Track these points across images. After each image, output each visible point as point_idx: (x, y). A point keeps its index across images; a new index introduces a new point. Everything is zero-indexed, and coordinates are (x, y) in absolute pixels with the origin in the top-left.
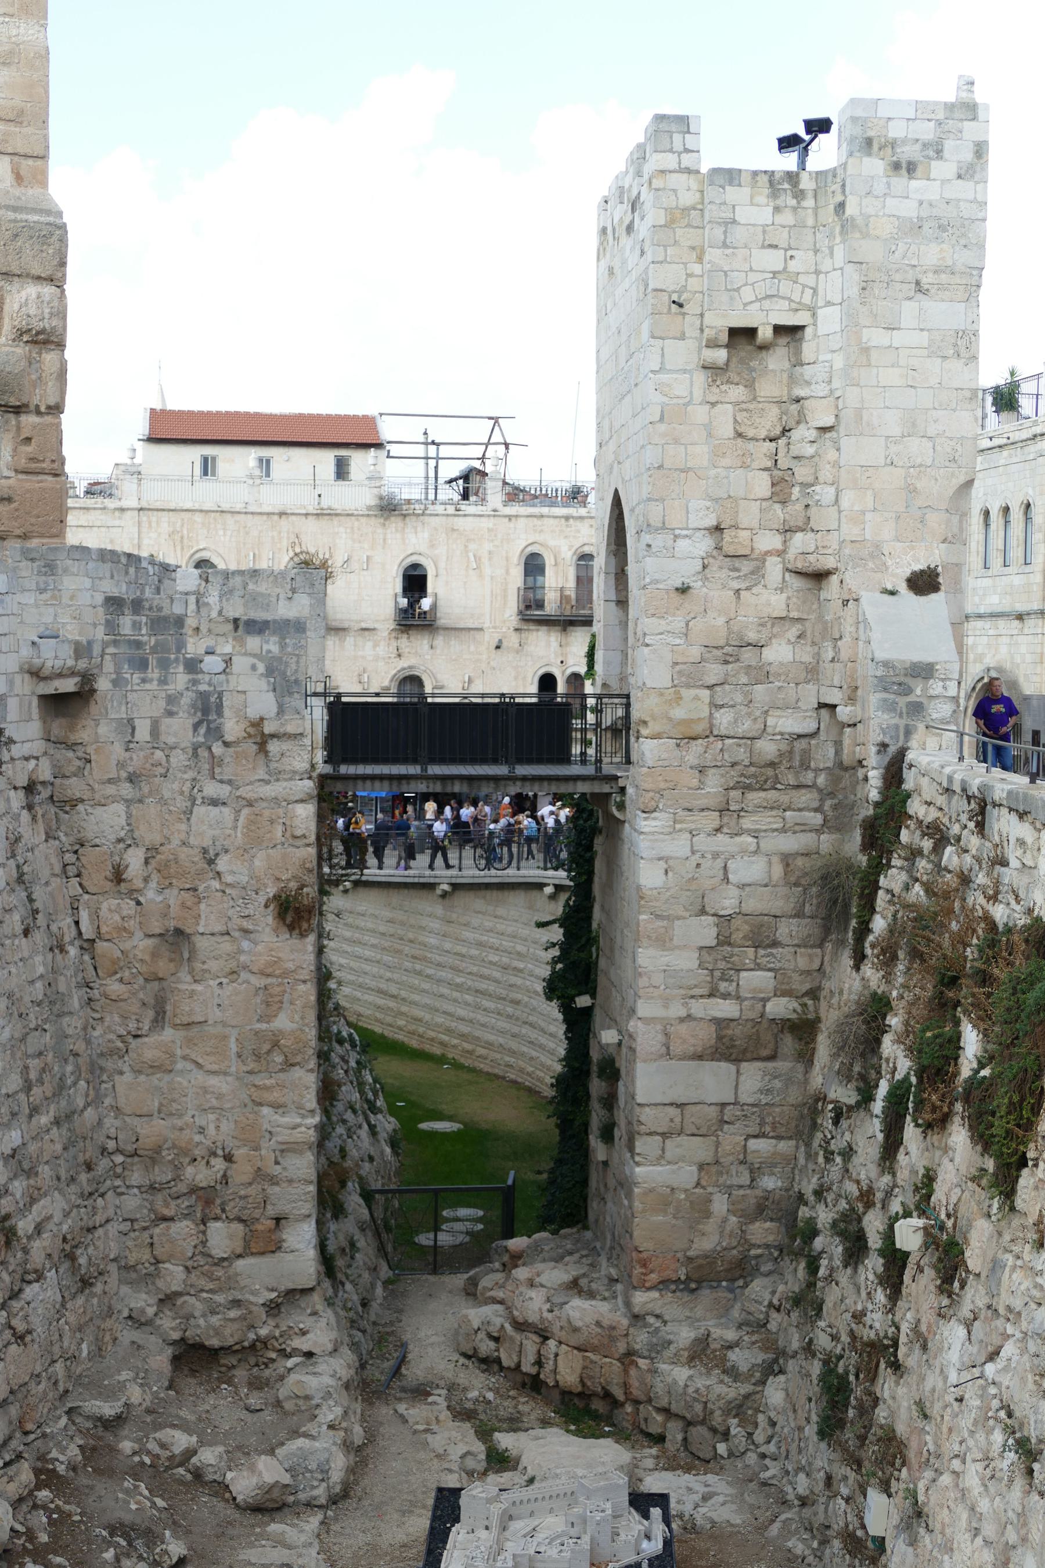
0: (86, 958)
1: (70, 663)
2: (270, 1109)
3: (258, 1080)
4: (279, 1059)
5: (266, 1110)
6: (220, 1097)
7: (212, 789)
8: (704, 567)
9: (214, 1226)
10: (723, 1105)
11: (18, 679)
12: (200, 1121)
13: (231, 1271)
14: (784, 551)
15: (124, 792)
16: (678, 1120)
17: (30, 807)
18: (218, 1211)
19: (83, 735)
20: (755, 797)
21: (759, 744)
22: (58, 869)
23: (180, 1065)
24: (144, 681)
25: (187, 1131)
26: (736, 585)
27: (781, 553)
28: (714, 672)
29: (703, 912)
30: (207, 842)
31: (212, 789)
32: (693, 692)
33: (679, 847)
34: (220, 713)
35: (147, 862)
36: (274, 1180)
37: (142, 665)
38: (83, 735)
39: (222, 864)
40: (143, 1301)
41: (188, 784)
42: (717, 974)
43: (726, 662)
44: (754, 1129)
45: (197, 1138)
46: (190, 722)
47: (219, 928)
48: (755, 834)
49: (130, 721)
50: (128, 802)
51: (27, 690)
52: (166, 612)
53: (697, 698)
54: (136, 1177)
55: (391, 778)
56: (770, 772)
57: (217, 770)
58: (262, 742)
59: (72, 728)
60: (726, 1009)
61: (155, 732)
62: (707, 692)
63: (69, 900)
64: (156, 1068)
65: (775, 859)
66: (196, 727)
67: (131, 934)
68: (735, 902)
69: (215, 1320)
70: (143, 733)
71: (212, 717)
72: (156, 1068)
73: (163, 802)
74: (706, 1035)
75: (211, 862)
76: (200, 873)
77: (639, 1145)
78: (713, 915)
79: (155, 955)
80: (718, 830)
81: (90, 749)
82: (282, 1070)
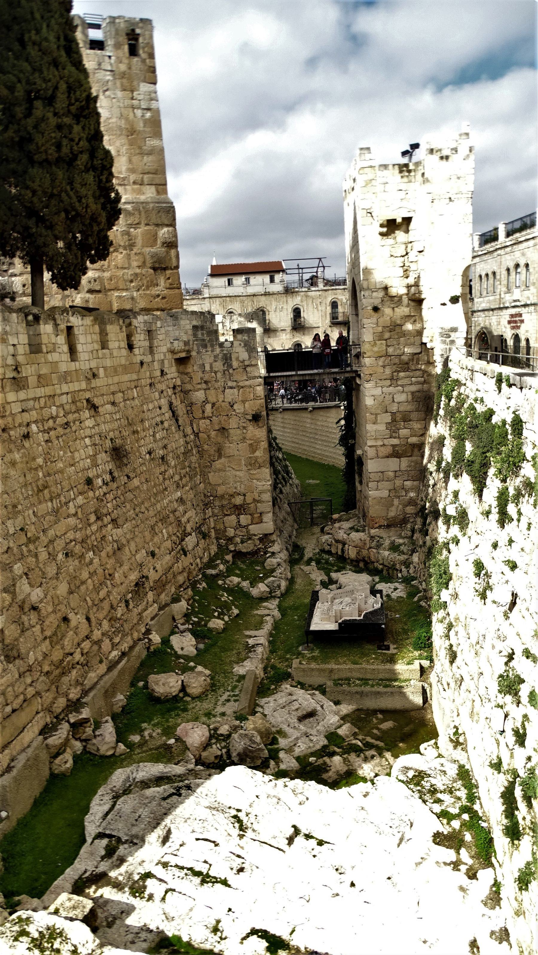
1: (183, 348)
3: (252, 472)
4: (257, 465)
5: (254, 481)
6: (240, 478)
7: (230, 384)
8: (382, 301)
9: (242, 516)
10: (396, 471)
12: (235, 485)
17: (175, 394)
19: (190, 370)
20: (402, 374)
21: (402, 357)
22: (185, 412)
23: (228, 469)
24: (207, 351)
26: (392, 306)
27: (407, 294)
28: (387, 335)
29: (387, 412)
30: (230, 400)
32: (380, 342)
33: (378, 391)
34: (231, 360)
35: (212, 408)
36: (258, 501)
37: (205, 346)
38: (190, 370)
39: (235, 407)
43: (391, 332)
44: (406, 478)
47: (236, 427)
48: (402, 386)
50: (205, 390)
51: (170, 357)
52: (211, 329)
53: (381, 344)
54: (217, 503)
56: (406, 366)
58: (245, 368)
59: (186, 368)
60: (395, 441)
61: (211, 367)
64: (220, 470)
65: (409, 394)
66: (224, 365)
68: (396, 408)
72: (220, 470)
74: (389, 450)
75: (232, 406)
76: (229, 410)
77: (370, 485)
79: (217, 436)
80: (390, 386)
81: (192, 374)
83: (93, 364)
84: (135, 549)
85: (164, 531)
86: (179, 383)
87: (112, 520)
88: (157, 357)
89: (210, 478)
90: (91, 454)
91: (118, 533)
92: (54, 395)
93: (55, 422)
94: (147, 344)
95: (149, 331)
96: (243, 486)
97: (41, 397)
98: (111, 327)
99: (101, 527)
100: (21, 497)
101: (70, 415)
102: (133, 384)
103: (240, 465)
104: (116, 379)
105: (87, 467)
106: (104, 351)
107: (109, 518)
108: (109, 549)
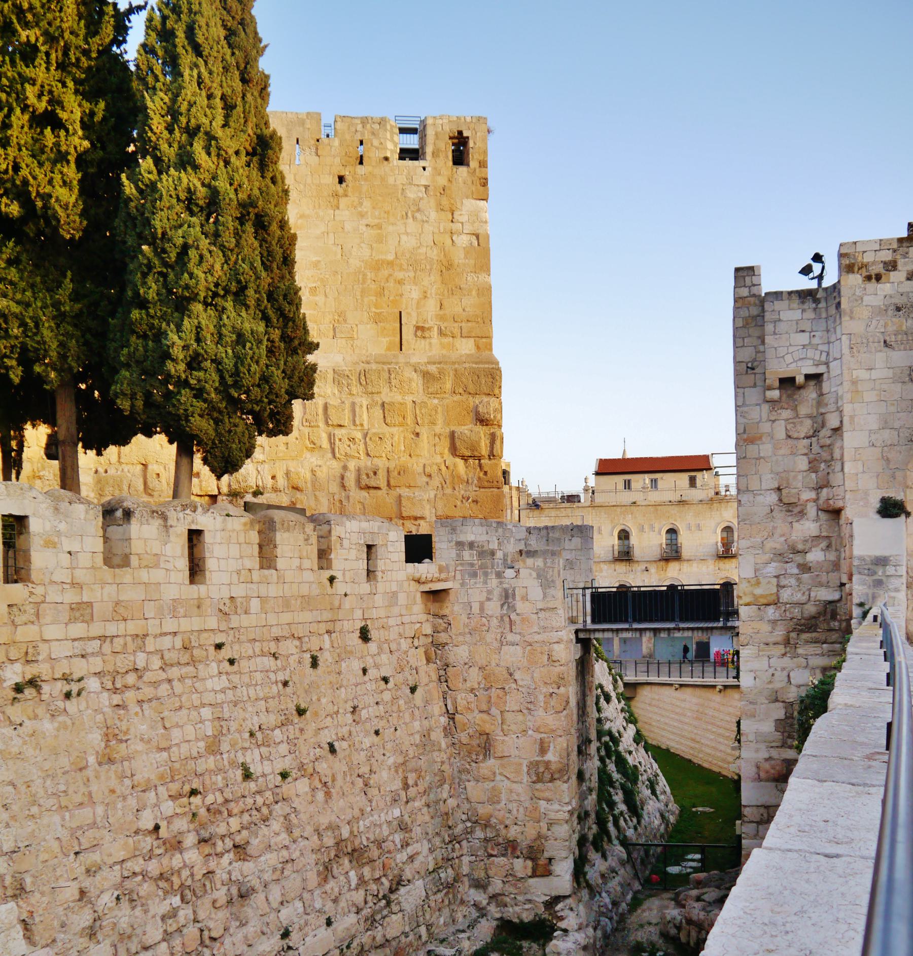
0: (451, 723)
1: (437, 575)
2: (545, 802)
11: (406, 584)
12: (510, 806)
13: (526, 884)
14: (818, 499)
15: (467, 639)
16: (765, 815)
18: (519, 853)
19: (446, 611)
20: (805, 636)
21: (806, 607)
23: (498, 778)
24: (476, 583)
25: (502, 812)
29: (777, 700)
31: (510, 637)
34: (514, 599)
37: (474, 575)
40: (481, 897)
41: (499, 635)
42: (786, 734)
45: (508, 815)
46: (499, 604)
47: (516, 708)
49: (469, 603)
52: (485, 548)
53: (769, 582)
55: (612, 630)
57: (513, 627)
59: (441, 608)
61: (482, 609)
62: (775, 579)
63: (441, 694)
66: (502, 606)
67: (473, 711)
69: (517, 909)
70: (476, 608)
71: (510, 600)
73: (487, 644)
75: (511, 675)
78: (783, 702)
80: (784, 655)
81: (450, 618)
82: (550, 782)
83: (239, 591)
84: (280, 900)
85: (352, 874)
86: (428, 629)
87: (235, 846)
88: (381, 587)
89: (469, 789)
90: (209, 733)
91: (244, 868)
92: (146, 636)
93: (140, 677)
94: (363, 565)
95: (369, 547)
96: (521, 810)
97: (117, 636)
98: (286, 535)
99: (210, 855)
100: (41, 792)
101: (175, 669)
102: (323, 628)
103: (518, 772)
104: (286, 618)
105: (195, 754)
106: (266, 572)
107: (229, 843)
108: (221, 895)
